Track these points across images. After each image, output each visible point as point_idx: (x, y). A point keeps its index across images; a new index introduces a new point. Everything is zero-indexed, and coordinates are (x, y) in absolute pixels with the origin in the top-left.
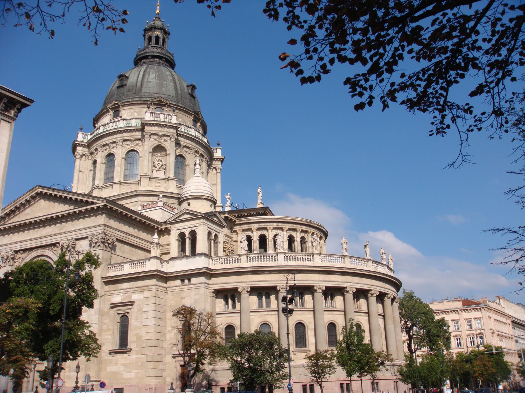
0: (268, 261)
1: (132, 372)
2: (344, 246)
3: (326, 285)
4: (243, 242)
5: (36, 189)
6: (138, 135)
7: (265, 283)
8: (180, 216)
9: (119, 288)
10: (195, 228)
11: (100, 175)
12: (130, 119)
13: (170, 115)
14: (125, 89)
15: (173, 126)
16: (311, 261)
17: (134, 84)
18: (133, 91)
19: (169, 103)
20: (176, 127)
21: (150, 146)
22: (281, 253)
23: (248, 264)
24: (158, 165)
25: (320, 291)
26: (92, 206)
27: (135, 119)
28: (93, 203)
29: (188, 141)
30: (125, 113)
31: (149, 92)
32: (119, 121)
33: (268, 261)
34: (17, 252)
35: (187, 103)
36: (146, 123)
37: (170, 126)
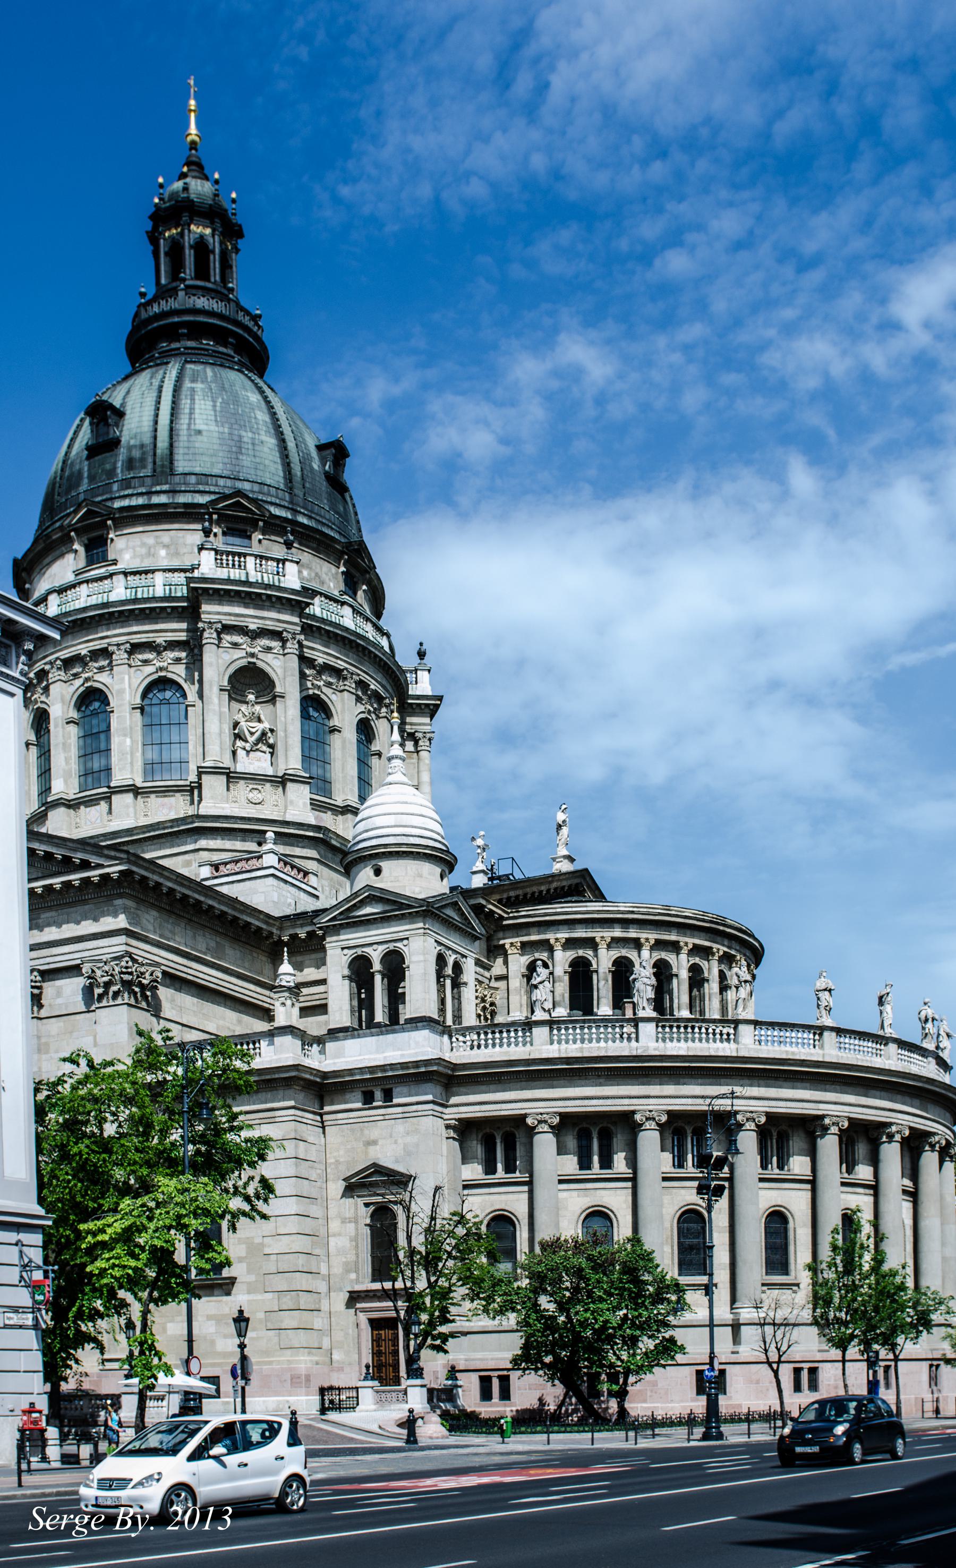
0: (610, 1042)
2: (823, 998)
3: (768, 1110)
4: (541, 986)
6: (177, 630)
10: (399, 945)
12: (146, 572)
16: (728, 1040)
17: (147, 440)
18: (144, 467)
21: (222, 669)
22: (648, 1020)
23: (552, 1051)
24: (252, 734)
25: (750, 1125)
27: (164, 571)
32: (111, 576)
33: (610, 1042)
35: (323, 512)
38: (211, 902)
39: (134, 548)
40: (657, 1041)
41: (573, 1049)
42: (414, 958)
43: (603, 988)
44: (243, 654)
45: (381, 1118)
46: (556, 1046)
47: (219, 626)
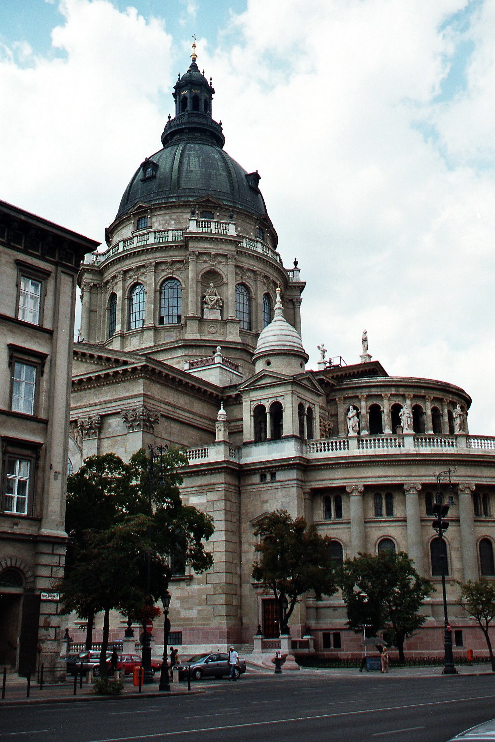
0: (389, 447)
1: (192, 609)
4: (352, 419)
7: (386, 479)
8: (257, 380)
12: (165, 231)
13: (226, 224)
14: (153, 185)
16: (453, 445)
19: (222, 204)
20: (235, 241)
22: (409, 435)
25: (467, 491)
26: (125, 368)
27: (173, 230)
28: (125, 363)
29: (252, 262)
31: (190, 187)
32: (149, 233)
33: (389, 447)
36: (191, 237)
37: (226, 240)
39: (159, 221)
40: (415, 447)
41: (370, 451)
42: (287, 406)
43: (386, 418)
44: (208, 265)
45: (270, 488)
46: (361, 449)
47: (197, 253)
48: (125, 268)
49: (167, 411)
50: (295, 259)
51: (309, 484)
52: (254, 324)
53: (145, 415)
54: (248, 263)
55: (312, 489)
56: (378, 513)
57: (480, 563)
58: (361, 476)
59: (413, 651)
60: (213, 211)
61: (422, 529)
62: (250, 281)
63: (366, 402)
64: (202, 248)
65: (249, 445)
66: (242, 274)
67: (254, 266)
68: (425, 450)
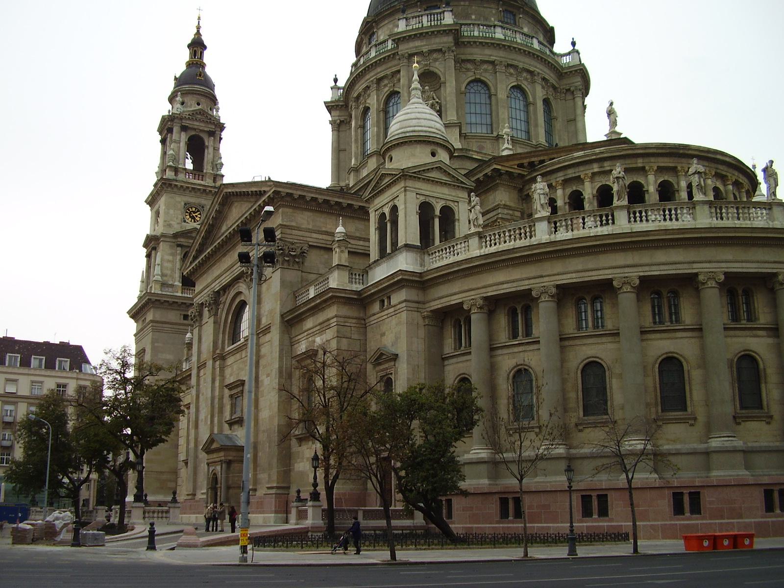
0: (518, 241)
3: (642, 274)
5: (222, 191)
8: (377, 183)
9: (305, 328)
10: (396, 201)
11: (357, 147)
12: (384, 42)
15: (444, 31)
22: (541, 219)
29: (487, 51)
30: (382, 35)
34: (218, 292)
36: (399, 39)
37: (438, 32)
38: (349, 202)
45: (386, 317)
47: (407, 55)
48: (355, 95)
49: (324, 242)
50: (573, 39)
51: (427, 305)
52: (494, 125)
53: (281, 249)
54: (478, 54)
55: (436, 312)
56: (515, 336)
57: (659, 394)
58: (479, 285)
59: (536, 525)
60: (439, 4)
61: (563, 349)
62: (487, 75)
63: (564, 189)
64: (413, 48)
65: (372, 266)
66: (476, 69)
67: (491, 56)
68: (563, 235)
